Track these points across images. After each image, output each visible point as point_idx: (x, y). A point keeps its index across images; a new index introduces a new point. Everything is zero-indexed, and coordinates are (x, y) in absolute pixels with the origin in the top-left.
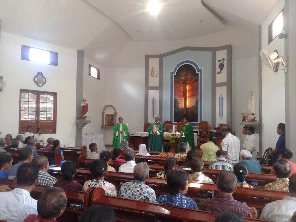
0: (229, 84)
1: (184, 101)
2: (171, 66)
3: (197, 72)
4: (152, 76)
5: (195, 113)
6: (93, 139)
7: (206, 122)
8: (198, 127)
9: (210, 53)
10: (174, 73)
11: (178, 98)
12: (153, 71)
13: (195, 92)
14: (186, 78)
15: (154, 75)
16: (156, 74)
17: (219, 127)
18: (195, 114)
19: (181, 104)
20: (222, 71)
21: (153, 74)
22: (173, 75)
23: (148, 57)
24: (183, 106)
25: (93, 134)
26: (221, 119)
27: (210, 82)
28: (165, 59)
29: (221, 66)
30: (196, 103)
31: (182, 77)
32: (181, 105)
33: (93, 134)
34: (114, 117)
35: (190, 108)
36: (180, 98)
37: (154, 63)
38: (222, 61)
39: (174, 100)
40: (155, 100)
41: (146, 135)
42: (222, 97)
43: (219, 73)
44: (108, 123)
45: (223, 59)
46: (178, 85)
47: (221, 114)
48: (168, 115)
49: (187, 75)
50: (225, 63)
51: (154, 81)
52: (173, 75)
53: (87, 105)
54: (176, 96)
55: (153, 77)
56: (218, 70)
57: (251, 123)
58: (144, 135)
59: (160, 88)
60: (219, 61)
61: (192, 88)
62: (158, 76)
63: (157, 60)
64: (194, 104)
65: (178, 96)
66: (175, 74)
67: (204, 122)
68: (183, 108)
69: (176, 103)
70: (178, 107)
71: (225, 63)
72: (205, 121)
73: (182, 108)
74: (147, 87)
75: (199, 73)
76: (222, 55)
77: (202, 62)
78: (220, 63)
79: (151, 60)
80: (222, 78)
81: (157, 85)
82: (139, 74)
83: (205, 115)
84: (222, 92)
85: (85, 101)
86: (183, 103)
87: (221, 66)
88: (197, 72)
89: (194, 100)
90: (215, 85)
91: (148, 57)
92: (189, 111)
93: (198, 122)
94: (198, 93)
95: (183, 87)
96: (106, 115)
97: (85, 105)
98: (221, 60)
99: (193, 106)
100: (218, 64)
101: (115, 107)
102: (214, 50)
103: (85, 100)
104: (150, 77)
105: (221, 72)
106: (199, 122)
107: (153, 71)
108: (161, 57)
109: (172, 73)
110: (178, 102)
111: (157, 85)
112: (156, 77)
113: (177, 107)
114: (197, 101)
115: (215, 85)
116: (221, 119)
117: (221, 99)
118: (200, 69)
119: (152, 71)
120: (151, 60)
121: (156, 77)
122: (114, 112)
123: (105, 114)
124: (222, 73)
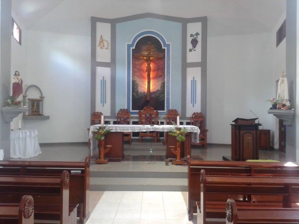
0: (203, 64)
1: (147, 83)
3: (163, 48)
4: (101, 48)
5: (160, 99)
6: (25, 138)
7: (175, 110)
8: (131, 115)
9: (180, 25)
10: (132, 45)
11: (138, 79)
12: (102, 41)
13: (161, 72)
14: (150, 53)
15: (104, 46)
16: (106, 44)
17: (192, 116)
18: (160, 100)
19: (141, 87)
20: (194, 48)
21: (102, 43)
22: (131, 48)
23: (94, 21)
24: (146, 90)
25: (20, 129)
26: (193, 106)
27: (179, 61)
28: (118, 26)
29: (194, 42)
30: (161, 86)
31: (143, 51)
32: (143, 87)
33: (20, 129)
34: (41, 103)
35: (154, 93)
36: (140, 79)
37: (104, 30)
38: (195, 36)
39: (132, 82)
40: (105, 81)
41: (131, 129)
42: (195, 80)
43: (191, 50)
44: (33, 112)
45: (197, 34)
46: (137, 63)
47: (193, 101)
48: (123, 102)
49: (148, 52)
50: (199, 38)
51: (104, 55)
52: (131, 48)
53: (22, 82)
54: (136, 77)
55: (102, 48)
56: (189, 46)
57: (280, 112)
58: (123, 129)
59: (112, 64)
60: (192, 36)
61: (156, 68)
62: (110, 47)
63: (108, 26)
64: (159, 88)
65: (138, 77)
66: (134, 48)
67: (172, 110)
68: (144, 92)
69: (135, 85)
70: (137, 92)
71: (199, 38)
72: (174, 109)
73: (142, 92)
74: (95, 64)
75: (166, 48)
76: (194, 28)
77: (170, 37)
78: (193, 38)
79: (99, 25)
80: (194, 56)
81: (108, 60)
82: (81, 43)
83: (173, 101)
84: (194, 74)
85: (19, 75)
86: (146, 87)
87: (194, 42)
88: (163, 48)
89: (160, 82)
90: (185, 66)
91: (94, 21)
92: (153, 96)
93: (132, 110)
94: (165, 74)
95: (147, 66)
96: (29, 99)
97: (17, 81)
98: (194, 34)
99: (158, 90)
100: (189, 39)
101: (41, 89)
102: (184, 22)
103: (17, 73)
104: (98, 49)
105: (194, 49)
106: (166, 111)
107: (102, 41)
108: (113, 22)
109: (129, 46)
110: (137, 84)
111: (108, 60)
112: (106, 49)
113: (137, 91)
114: (164, 84)
115: (185, 66)
116: (193, 106)
117: (194, 82)
118: (167, 43)
119: (101, 40)
120: (99, 25)
121: (106, 49)
122: (40, 95)
123: (27, 98)
124: (195, 50)
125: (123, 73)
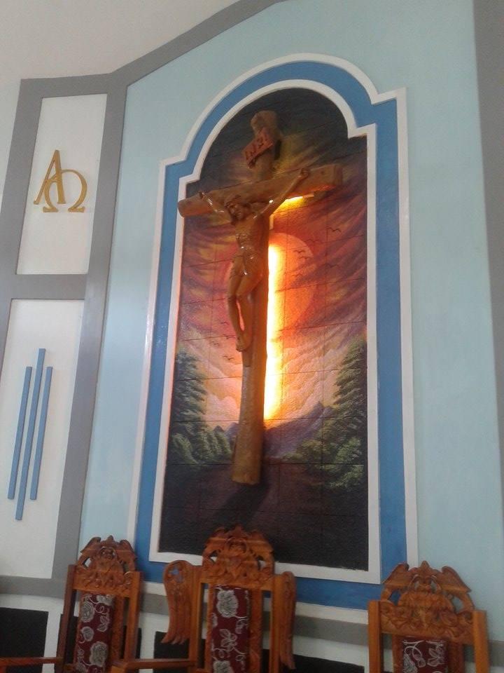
2: (174, 129)
3: (353, 131)
5: (336, 477)
7: (447, 570)
10: (186, 167)
13: (339, 287)
15: (62, 200)
16: (73, 188)
18: (333, 485)
19: (221, 397)
21: (54, 189)
28: (137, 93)
30: (341, 383)
35: (291, 429)
36: (218, 345)
39: (176, 364)
52: (184, 181)
54: (196, 334)
55: (53, 210)
62: (90, 203)
64: (326, 393)
66: (195, 176)
67: (425, 571)
69: (187, 387)
70: (198, 424)
72: (437, 565)
75: (370, 132)
81: (77, 263)
88: (353, 131)
92: (288, 452)
93: (362, 564)
99: (319, 409)
106: (373, 574)
108: (114, 88)
109: (173, 173)
110: (199, 379)
111: (77, 263)
113: (199, 419)
114: (359, 362)
118: (376, 98)
119: (53, 172)
125: (135, 323)
